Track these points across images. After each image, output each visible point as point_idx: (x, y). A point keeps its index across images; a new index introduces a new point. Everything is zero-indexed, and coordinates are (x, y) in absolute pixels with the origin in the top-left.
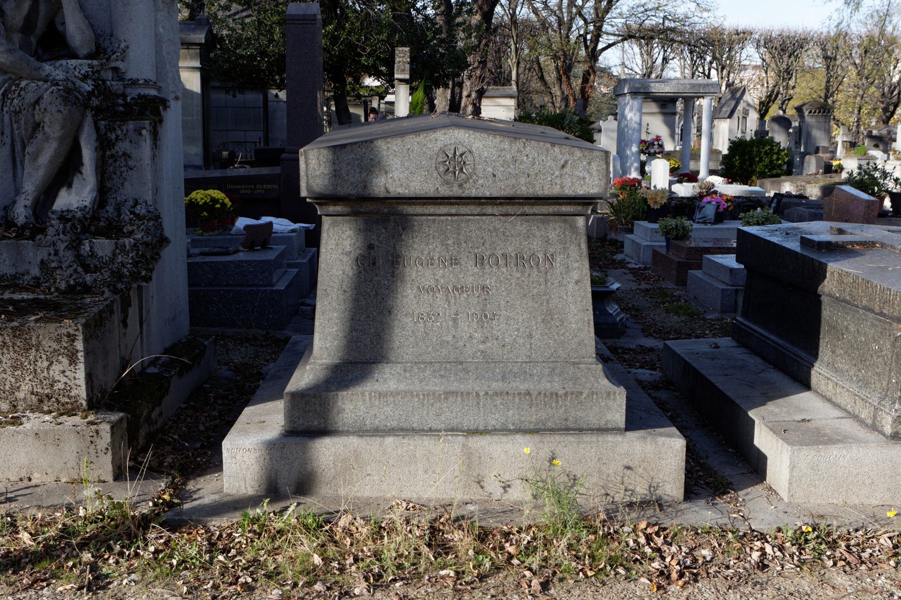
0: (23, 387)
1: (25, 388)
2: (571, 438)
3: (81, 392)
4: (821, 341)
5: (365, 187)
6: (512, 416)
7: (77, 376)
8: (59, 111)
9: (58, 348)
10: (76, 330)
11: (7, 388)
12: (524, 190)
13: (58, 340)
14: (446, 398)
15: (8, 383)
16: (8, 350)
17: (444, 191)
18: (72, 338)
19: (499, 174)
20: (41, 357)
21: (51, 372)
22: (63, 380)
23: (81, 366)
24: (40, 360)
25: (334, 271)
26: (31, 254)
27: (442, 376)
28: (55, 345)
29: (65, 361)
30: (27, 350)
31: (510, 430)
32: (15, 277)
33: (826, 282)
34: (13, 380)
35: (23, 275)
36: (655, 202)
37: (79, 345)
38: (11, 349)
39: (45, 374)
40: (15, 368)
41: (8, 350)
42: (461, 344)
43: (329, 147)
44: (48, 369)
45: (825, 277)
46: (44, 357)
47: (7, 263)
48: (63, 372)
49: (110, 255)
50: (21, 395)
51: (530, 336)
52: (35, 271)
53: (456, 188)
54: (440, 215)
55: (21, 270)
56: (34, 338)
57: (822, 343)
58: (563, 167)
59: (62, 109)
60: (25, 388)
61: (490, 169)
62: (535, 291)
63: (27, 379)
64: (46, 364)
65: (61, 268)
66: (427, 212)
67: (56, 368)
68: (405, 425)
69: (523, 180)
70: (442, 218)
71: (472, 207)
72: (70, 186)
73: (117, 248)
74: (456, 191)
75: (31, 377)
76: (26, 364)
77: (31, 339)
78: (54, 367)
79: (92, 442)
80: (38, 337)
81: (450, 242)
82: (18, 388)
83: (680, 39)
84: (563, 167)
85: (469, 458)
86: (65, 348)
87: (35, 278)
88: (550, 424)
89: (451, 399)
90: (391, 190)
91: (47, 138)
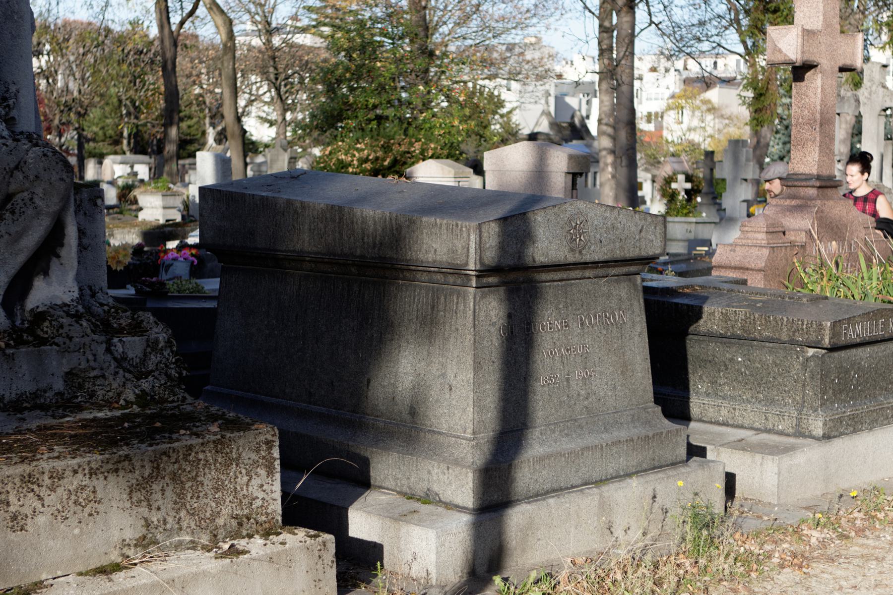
0: (223, 512)
1: (226, 511)
2: (660, 475)
3: (276, 507)
4: (691, 376)
5: (520, 257)
6: (621, 462)
7: (274, 488)
8: (62, 179)
9: (257, 458)
10: (273, 436)
11: (208, 515)
12: (618, 254)
13: (258, 450)
14: (582, 454)
15: (209, 509)
16: (210, 469)
17: (571, 258)
18: (269, 443)
19: (603, 240)
20: (241, 473)
21: (250, 489)
22: (261, 495)
23: (278, 476)
24: (240, 476)
25: (485, 342)
26: (54, 363)
27: (567, 435)
28: (254, 456)
29: (262, 472)
30: (228, 466)
31: (621, 476)
32: (35, 395)
33: (701, 322)
34: (214, 505)
35: (45, 391)
36: (119, 262)
37: (276, 453)
38: (213, 467)
39: (245, 492)
40: (217, 489)
41: (210, 469)
42: (573, 402)
43: (496, 220)
44: (247, 485)
45: (700, 317)
46: (244, 471)
47: (26, 377)
48: (262, 486)
49: (141, 355)
50: (220, 521)
51: (615, 388)
52: (59, 385)
53: (577, 255)
54: (554, 281)
55: (43, 385)
56: (234, 451)
57: (693, 379)
58: (641, 231)
59: (64, 177)
60: (226, 511)
61: (598, 236)
62: (616, 345)
63: (228, 500)
64: (246, 478)
65: (103, 376)
66: (556, 278)
67: (255, 482)
68: (555, 486)
69: (618, 245)
70: (555, 283)
71: (577, 272)
72: (46, 273)
73: (148, 346)
74: (577, 258)
75: (231, 497)
76: (227, 482)
77: (231, 452)
78: (253, 482)
79: (320, 557)
80: (238, 450)
81: (561, 306)
82: (219, 513)
83: (271, 70)
84: (641, 231)
85: (604, 506)
86: (264, 458)
87: (60, 394)
88: (645, 466)
89: (585, 454)
90: (537, 259)
91: (38, 213)
